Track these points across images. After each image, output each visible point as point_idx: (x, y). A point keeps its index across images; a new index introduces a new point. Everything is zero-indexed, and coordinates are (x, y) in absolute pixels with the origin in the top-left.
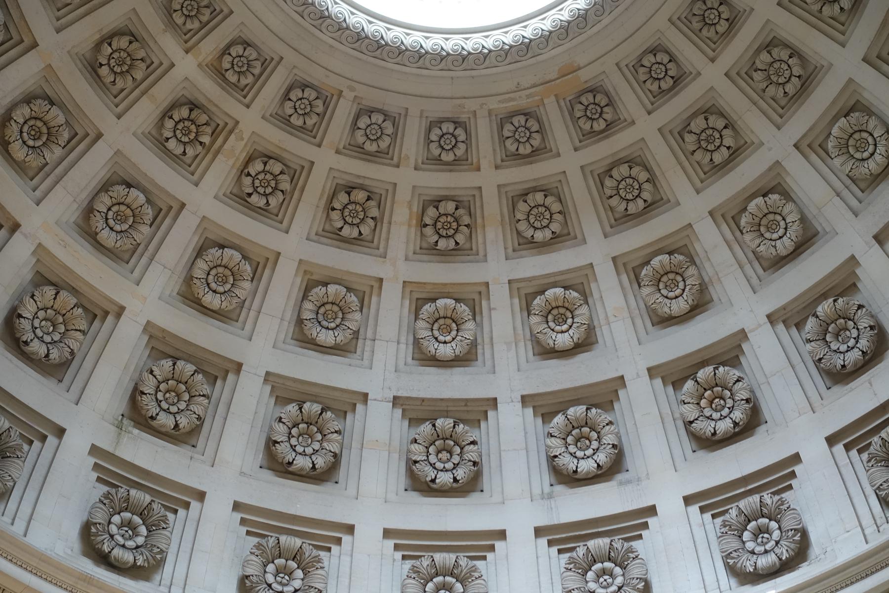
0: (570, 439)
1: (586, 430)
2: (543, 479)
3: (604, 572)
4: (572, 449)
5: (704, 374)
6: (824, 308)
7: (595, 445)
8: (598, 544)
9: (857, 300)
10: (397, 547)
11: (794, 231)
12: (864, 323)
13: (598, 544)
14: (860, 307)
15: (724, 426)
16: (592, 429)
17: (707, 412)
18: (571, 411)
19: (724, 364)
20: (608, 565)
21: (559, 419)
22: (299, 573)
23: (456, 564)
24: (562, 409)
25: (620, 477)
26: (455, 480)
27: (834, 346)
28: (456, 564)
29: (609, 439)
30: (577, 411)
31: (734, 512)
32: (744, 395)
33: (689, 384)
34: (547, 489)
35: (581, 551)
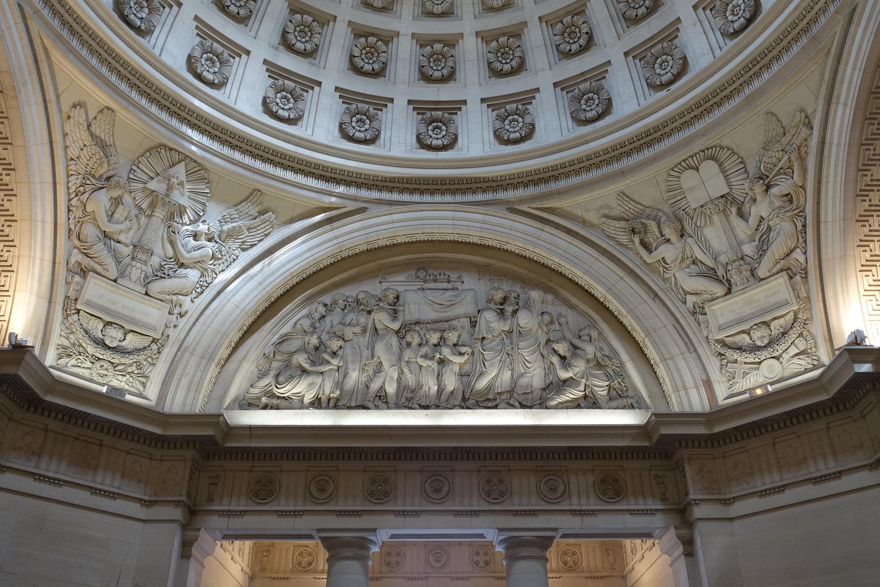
0: (298, 29)
1: (307, 29)
2: (276, 39)
3: (285, 97)
4: (296, 33)
5: (372, 40)
6: (438, 47)
7: (307, 38)
8: (289, 84)
9: (452, 52)
10: (197, 27)
11: (445, 6)
12: (450, 64)
13: (289, 84)
14: (452, 56)
15: (368, 67)
16: (310, 31)
17: (363, 57)
18: (305, 17)
19: (382, 41)
20: (289, 95)
21: (298, 16)
22: (146, 10)
23: (222, 54)
24: (302, 12)
25: (310, 59)
26: (238, 13)
27: (432, 64)
28: (222, 54)
29: (316, 40)
30: (308, 19)
31: (354, 106)
32: (384, 60)
33: (363, 40)
34: (276, 44)
35: (280, 82)
